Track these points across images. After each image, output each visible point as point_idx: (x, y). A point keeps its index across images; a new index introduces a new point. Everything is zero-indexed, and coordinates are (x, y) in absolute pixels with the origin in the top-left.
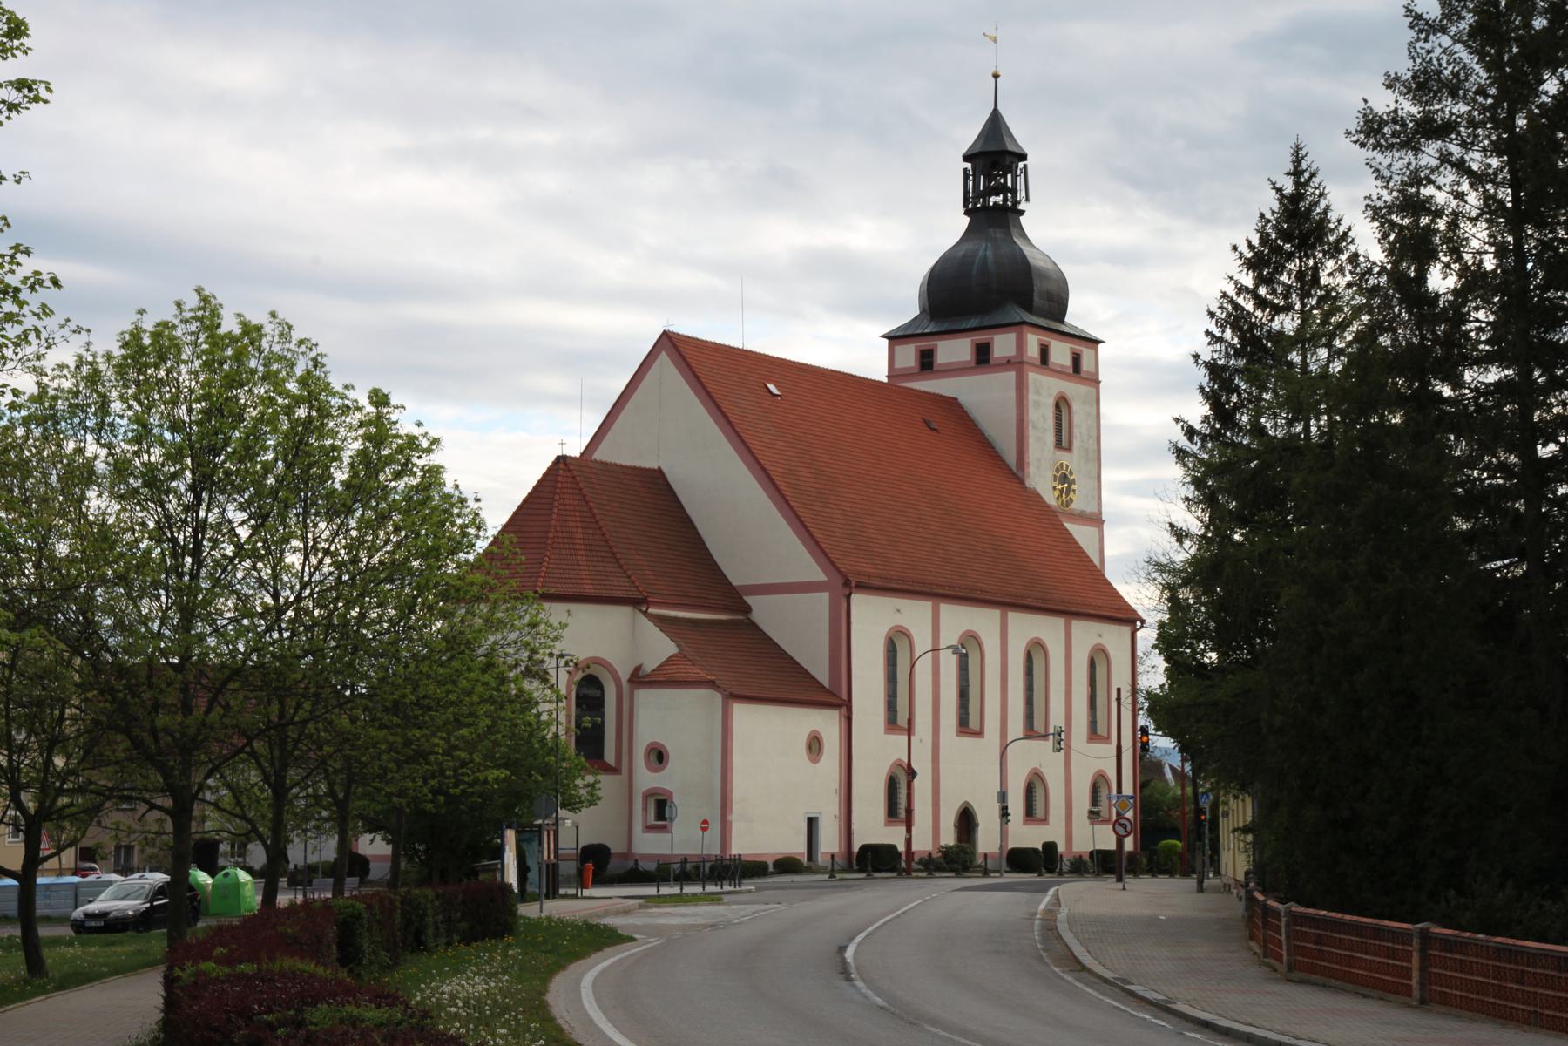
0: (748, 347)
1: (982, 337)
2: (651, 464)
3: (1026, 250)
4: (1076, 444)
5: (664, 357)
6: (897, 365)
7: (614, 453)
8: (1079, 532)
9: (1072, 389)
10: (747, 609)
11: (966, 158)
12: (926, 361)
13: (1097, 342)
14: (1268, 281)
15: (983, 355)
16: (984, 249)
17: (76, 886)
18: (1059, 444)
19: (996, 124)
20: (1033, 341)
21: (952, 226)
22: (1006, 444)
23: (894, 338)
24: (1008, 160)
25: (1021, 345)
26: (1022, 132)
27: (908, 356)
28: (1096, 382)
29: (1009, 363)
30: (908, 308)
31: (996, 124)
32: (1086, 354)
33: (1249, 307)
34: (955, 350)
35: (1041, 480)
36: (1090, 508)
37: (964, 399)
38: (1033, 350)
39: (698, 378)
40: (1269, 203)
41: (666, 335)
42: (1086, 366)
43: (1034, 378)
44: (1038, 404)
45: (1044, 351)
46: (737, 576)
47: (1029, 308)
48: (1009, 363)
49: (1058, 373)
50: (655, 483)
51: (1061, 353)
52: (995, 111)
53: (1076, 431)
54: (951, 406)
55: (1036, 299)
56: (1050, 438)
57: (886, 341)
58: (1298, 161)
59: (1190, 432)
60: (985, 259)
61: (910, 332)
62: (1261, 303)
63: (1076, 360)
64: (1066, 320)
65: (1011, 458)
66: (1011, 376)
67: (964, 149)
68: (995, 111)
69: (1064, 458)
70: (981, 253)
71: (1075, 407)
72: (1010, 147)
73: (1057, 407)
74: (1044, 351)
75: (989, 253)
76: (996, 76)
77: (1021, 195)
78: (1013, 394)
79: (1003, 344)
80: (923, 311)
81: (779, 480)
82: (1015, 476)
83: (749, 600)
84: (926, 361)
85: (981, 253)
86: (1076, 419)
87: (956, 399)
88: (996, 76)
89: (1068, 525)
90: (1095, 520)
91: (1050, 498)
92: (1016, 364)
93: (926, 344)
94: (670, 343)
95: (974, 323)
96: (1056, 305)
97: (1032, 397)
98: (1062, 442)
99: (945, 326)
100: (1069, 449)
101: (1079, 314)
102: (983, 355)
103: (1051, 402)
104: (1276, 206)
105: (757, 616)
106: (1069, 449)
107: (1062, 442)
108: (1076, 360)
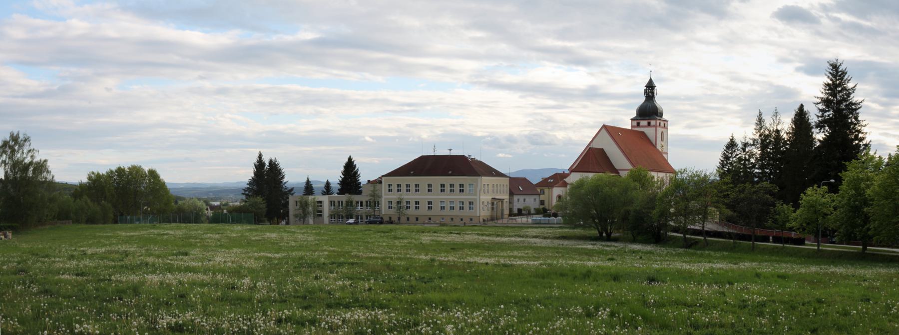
0: (615, 126)
1: (649, 121)
2: (601, 147)
3: (656, 104)
4: (664, 140)
5: (603, 130)
7: (594, 146)
8: (665, 155)
9: (664, 130)
10: (619, 173)
12: (638, 124)
15: (649, 124)
16: (649, 104)
18: (662, 140)
19: (651, 81)
20: (658, 122)
21: (642, 99)
22: (653, 139)
23: (632, 120)
25: (656, 122)
26: (656, 84)
27: (635, 123)
28: (667, 128)
29: (654, 126)
30: (634, 114)
31: (651, 81)
34: (644, 123)
35: (659, 147)
37: (645, 132)
38: (658, 124)
42: (666, 126)
45: (660, 123)
46: (617, 168)
47: (657, 116)
48: (654, 126)
51: (662, 124)
54: (643, 133)
63: (664, 125)
65: (654, 143)
66: (654, 128)
67: (645, 85)
69: (662, 143)
71: (664, 133)
74: (660, 123)
77: (655, 94)
79: (653, 122)
80: (637, 114)
82: (655, 146)
84: (638, 124)
90: (667, 153)
91: (660, 150)
92: (655, 126)
93: (638, 121)
94: (604, 126)
95: (647, 118)
97: (658, 132)
98: (662, 140)
99: (642, 118)
101: (665, 117)
102: (649, 124)
105: (620, 174)
107: (662, 140)
108: (664, 125)
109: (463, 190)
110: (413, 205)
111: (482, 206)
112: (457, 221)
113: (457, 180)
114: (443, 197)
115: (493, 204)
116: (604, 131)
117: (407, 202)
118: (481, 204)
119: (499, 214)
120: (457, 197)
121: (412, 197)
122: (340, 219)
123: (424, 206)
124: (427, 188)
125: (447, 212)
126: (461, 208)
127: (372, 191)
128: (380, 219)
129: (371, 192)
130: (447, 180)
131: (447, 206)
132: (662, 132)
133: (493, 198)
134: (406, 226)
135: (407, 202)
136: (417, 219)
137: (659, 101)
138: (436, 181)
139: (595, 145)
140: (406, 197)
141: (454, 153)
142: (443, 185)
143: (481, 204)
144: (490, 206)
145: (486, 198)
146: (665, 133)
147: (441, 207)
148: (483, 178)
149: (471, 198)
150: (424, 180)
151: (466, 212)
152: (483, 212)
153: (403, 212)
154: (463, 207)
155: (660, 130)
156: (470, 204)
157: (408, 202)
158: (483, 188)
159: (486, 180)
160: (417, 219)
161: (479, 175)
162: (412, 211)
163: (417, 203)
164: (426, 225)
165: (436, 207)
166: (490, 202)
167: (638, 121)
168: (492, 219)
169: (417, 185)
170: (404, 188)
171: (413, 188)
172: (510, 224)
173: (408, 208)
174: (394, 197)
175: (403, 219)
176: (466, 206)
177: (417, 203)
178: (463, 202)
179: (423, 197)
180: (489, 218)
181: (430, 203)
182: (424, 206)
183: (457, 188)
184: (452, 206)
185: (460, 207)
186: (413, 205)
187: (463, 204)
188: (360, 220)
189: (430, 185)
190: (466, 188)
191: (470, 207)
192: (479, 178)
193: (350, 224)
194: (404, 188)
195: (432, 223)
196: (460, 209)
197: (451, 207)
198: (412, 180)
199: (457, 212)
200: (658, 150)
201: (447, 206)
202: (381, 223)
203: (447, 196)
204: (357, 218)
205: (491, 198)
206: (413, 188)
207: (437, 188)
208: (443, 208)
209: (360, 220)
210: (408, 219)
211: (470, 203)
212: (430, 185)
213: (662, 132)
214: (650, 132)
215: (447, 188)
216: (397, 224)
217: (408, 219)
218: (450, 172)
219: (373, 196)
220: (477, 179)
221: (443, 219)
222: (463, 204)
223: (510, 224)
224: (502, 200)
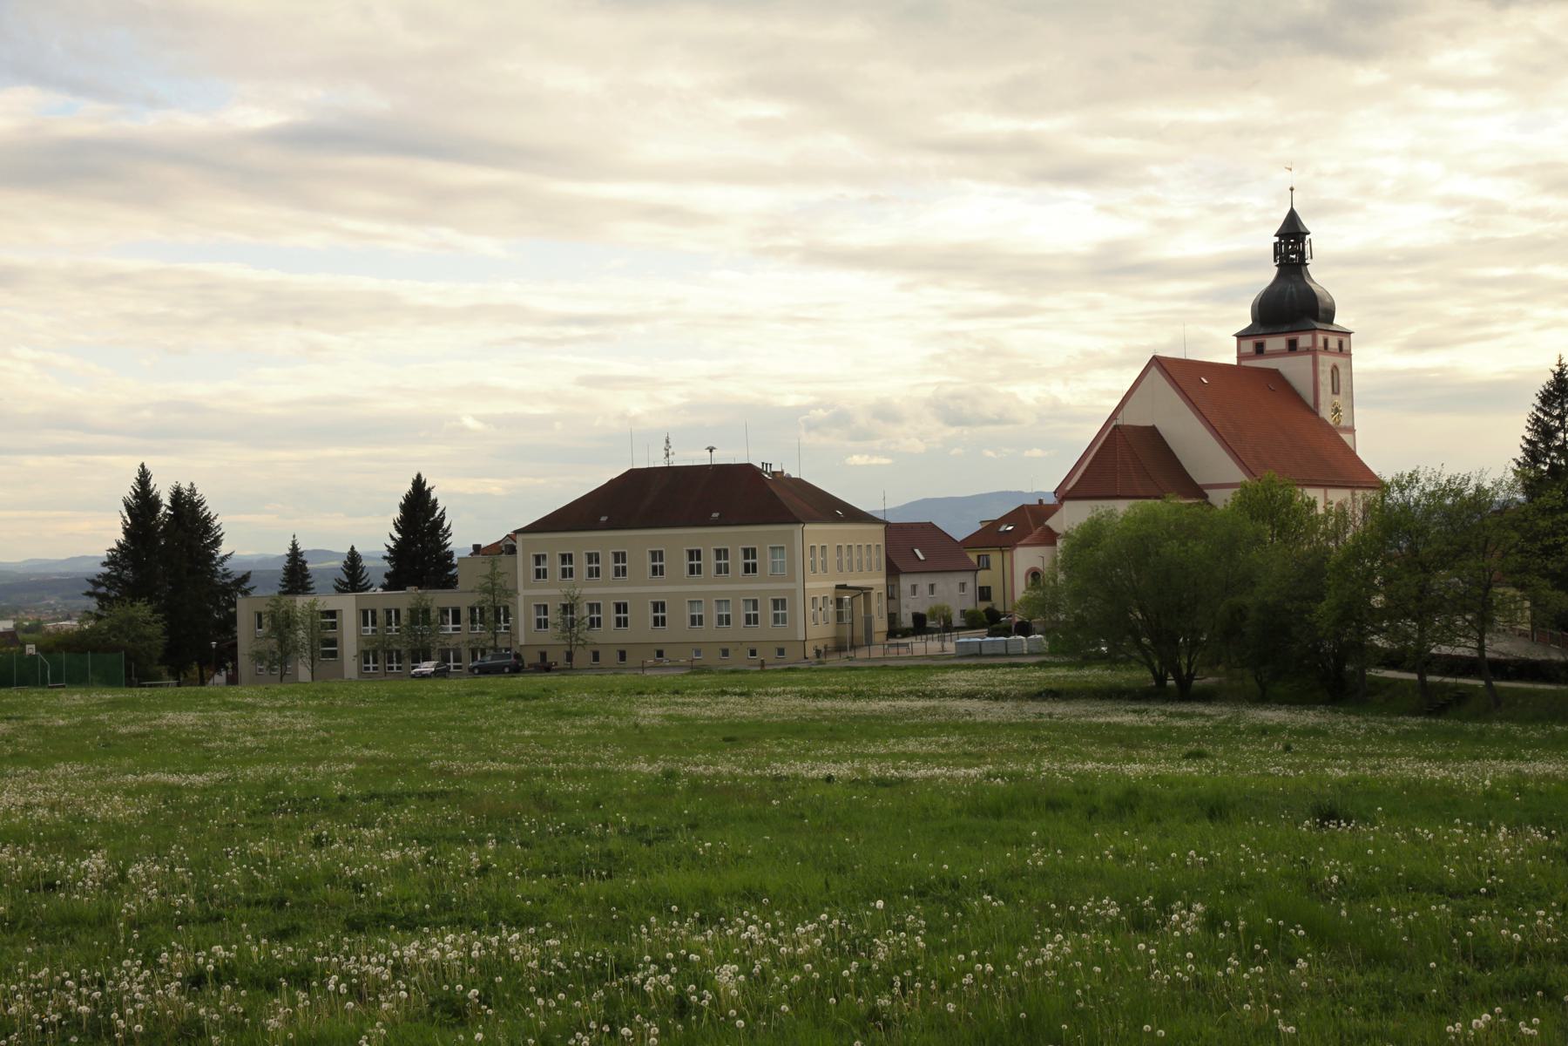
1: (1292, 336)
4: (1342, 390)
5: (1154, 369)
6: (1243, 351)
7: (1128, 419)
8: (1345, 437)
9: (1339, 360)
10: (1206, 496)
11: (1276, 235)
12: (1260, 350)
13: (1349, 333)
14: (1550, 406)
15: (1292, 346)
16: (1291, 288)
17: (1006, 641)
18: (1333, 392)
19: (1292, 218)
20: (1320, 337)
21: (1268, 274)
23: (1241, 336)
24: (1301, 236)
25: (1314, 341)
26: (1307, 222)
27: (1249, 346)
28: (1349, 355)
29: (1307, 351)
30: (1246, 321)
31: (1292, 218)
32: (1345, 340)
33: (1542, 416)
34: (1276, 343)
35: (1326, 413)
36: (1349, 424)
38: (1320, 343)
39: (1173, 380)
40: (1551, 377)
41: (1154, 357)
42: (1345, 347)
43: (1322, 358)
44: (1323, 371)
46: (1199, 480)
47: (1317, 319)
48: (1307, 351)
49: (1333, 353)
50: (1151, 434)
51: (1333, 342)
52: (1292, 208)
53: (1341, 383)
54: (1275, 374)
55: (1320, 314)
56: (1330, 388)
57: (1235, 338)
58: (1560, 361)
59: (1519, 464)
60: (1292, 293)
61: (1249, 333)
62: (1546, 414)
64: (1335, 322)
65: (1310, 401)
66: (1309, 357)
67: (1275, 232)
68: (1292, 208)
69: (1337, 399)
70: (1289, 290)
71: (1341, 370)
72: (1302, 230)
73: (1332, 372)
75: (1294, 290)
76: (1292, 189)
77: (1308, 255)
78: (1311, 368)
79: (1304, 340)
80: (1254, 319)
81: (1220, 431)
82: (1313, 411)
83: (1207, 491)
84: (1260, 350)
85: (1289, 290)
86: (1341, 377)
87: (1277, 370)
88: (1292, 189)
89: (1342, 435)
90: (1351, 430)
91: (1331, 421)
92: (1312, 351)
93: (1259, 340)
94: (1157, 362)
95: (1287, 328)
96: (1329, 315)
97: (1321, 368)
98: (1336, 391)
99: (1269, 331)
100: (1338, 393)
101: (1340, 321)
103: (1329, 369)
104: (1552, 378)
105: (1211, 499)
106: (1338, 393)
107: (1335, 391)
109: (754, 565)
110: (609, 615)
111: (810, 610)
112: (738, 659)
113: (735, 537)
114: (696, 587)
115: (839, 602)
116: (1156, 377)
117: (591, 606)
118: (809, 602)
119: (860, 631)
120: (738, 586)
121: (606, 590)
122: (391, 661)
123: (641, 617)
124: (649, 564)
125: (710, 631)
126: (751, 620)
127: (487, 577)
128: (512, 659)
129: (483, 581)
130: (707, 538)
131: (711, 614)
132: (1335, 369)
133: (838, 587)
134: (592, 678)
135: (591, 606)
136: (623, 656)
137: (1320, 275)
138: (676, 540)
139: (1130, 419)
140: (590, 591)
141: (723, 457)
142: (694, 554)
143: (809, 602)
144: (831, 608)
145: (821, 585)
146: (1341, 370)
147: (693, 618)
148: (808, 527)
149: (777, 588)
150: (638, 542)
151: (766, 629)
152: (816, 628)
153: (580, 635)
154: (756, 616)
155: (1326, 362)
156: (776, 607)
157: (594, 607)
158: (808, 559)
159: (816, 533)
160: (623, 656)
161: (798, 522)
162: (608, 633)
163: (621, 608)
164: (648, 673)
165: (678, 618)
166: (831, 596)
167: (1259, 340)
168: (839, 648)
169: (620, 557)
170: (581, 566)
171: (607, 565)
172: (890, 659)
173: (596, 623)
174: (553, 591)
175: (582, 657)
176: (766, 612)
177: (621, 608)
178: (755, 602)
179: (639, 589)
180: (831, 644)
181: (660, 606)
182: (641, 617)
183: (737, 561)
184: (724, 613)
185: (748, 616)
186: (609, 615)
187: (755, 608)
188: (452, 664)
189: (658, 556)
190: (764, 560)
191: (776, 616)
192: (797, 528)
193: (423, 676)
194: (581, 566)
195: (668, 667)
196: (748, 622)
197: (720, 617)
198: (606, 541)
199: (738, 631)
200: (1324, 421)
201: (711, 614)
202: (517, 669)
203: (708, 586)
204: (445, 659)
205: (833, 584)
206: (607, 565)
207: (677, 562)
208: (696, 620)
209: (452, 664)
210: (596, 656)
211: (776, 603)
212: (658, 556)
213: (1335, 369)
214: (1294, 369)
215: (709, 562)
216: (563, 671)
217: (596, 656)
218: (715, 515)
219: (491, 591)
220: (792, 532)
221: (698, 653)
222: (755, 608)
223: (890, 659)
224: (865, 592)
